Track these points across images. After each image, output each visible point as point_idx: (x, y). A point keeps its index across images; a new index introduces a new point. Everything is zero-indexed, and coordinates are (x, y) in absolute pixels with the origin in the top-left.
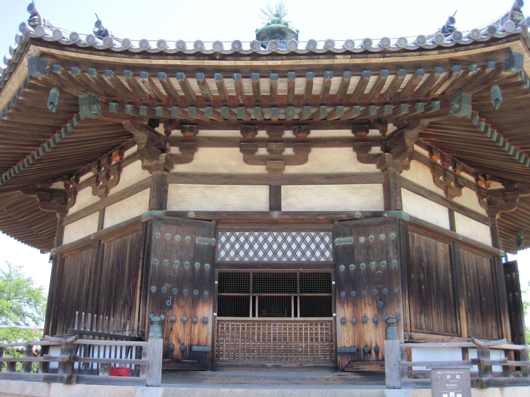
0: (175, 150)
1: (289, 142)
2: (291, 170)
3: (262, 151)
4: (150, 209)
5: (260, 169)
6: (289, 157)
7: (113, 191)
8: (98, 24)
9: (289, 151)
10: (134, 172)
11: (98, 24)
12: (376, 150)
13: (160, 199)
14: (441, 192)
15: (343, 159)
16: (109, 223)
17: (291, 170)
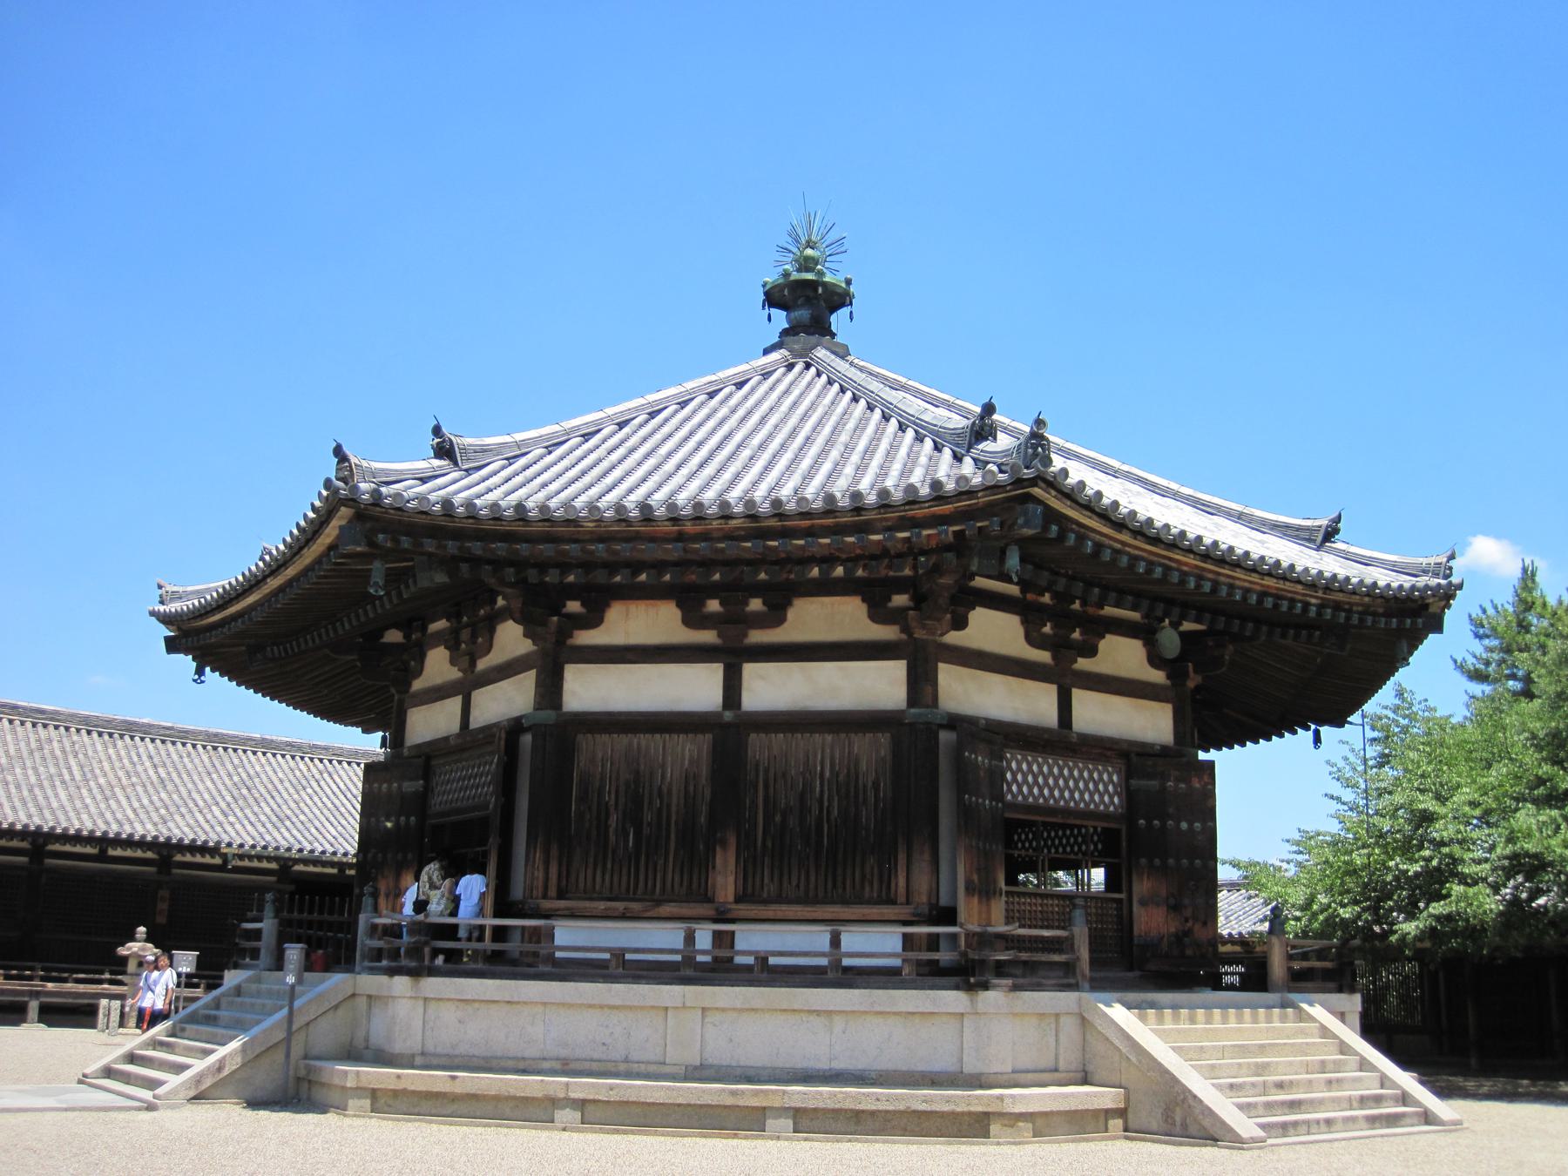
0: (574, 606)
1: (757, 590)
2: (757, 637)
3: (714, 605)
4: (539, 706)
5: (708, 637)
6: (756, 614)
7: (482, 664)
8: (437, 431)
9: (756, 604)
10: (511, 639)
11: (437, 431)
12: (900, 600)
13: (550, 689)
14: (1044, 656)
15: (842, 617)
16: (479, 718)
17: (757, 637)
